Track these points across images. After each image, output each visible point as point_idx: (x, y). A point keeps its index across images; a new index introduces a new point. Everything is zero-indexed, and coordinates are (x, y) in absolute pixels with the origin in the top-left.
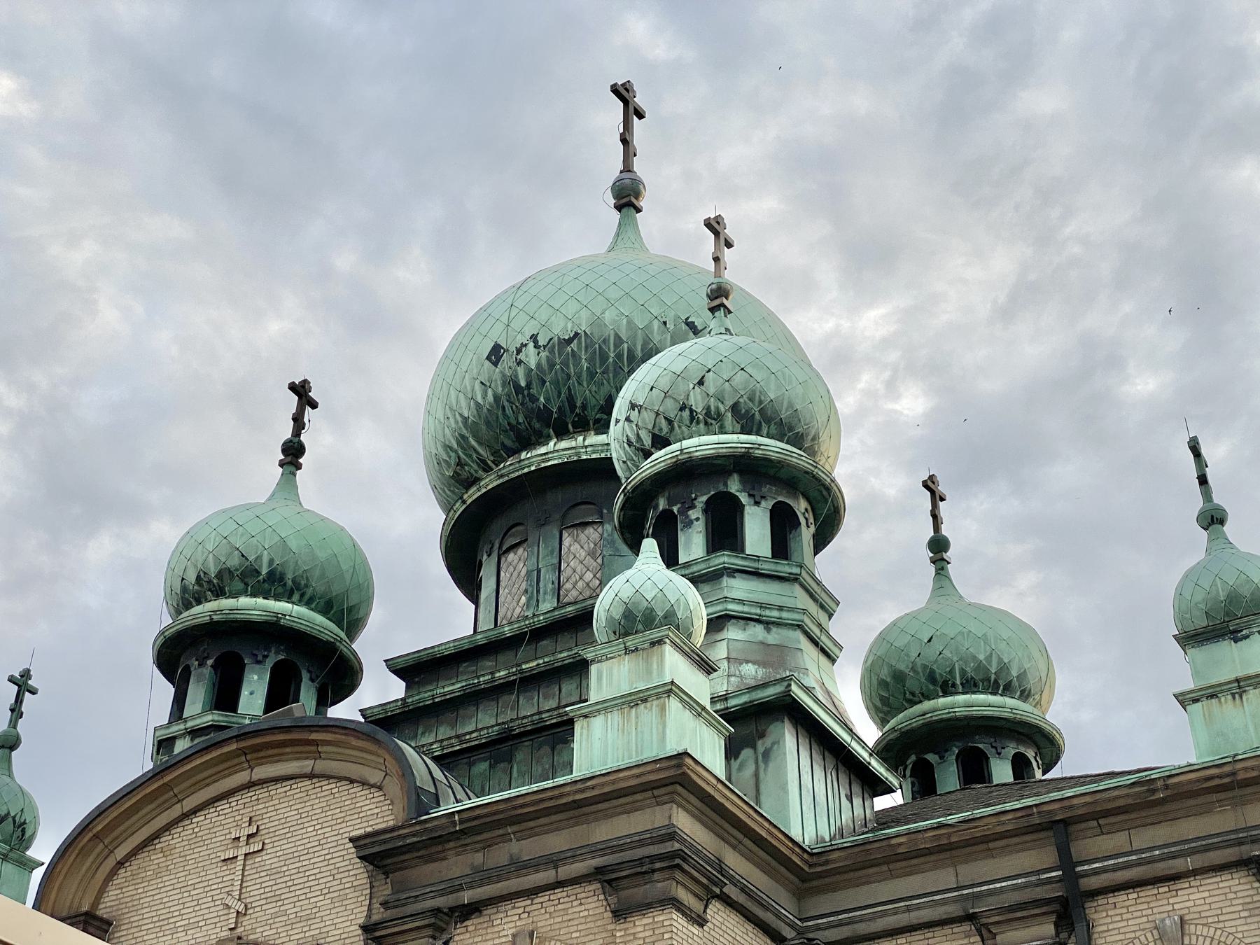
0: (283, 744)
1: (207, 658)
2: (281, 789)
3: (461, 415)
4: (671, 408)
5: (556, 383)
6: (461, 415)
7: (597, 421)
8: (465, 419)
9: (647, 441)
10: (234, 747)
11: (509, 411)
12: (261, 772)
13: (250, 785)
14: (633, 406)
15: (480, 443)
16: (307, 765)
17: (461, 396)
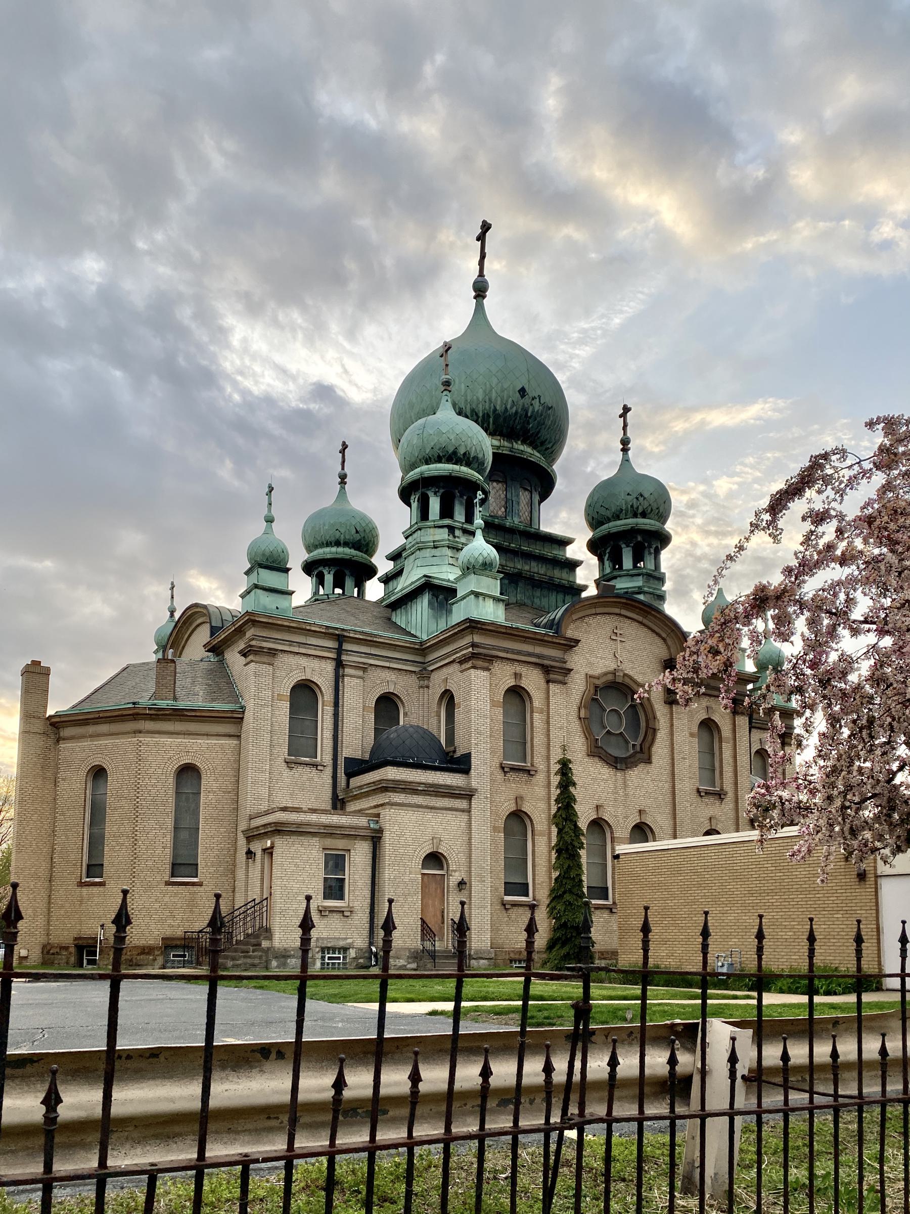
0: (637, 608)
1: (464, 495)
2: (629, 621)
3: (494, 407)
4: (655, 506)
5: (539, 423)
6: (494, 407)
7: (536, 445)
8: (495, 410)
9: (640, 510)
10: (625, 601)
11: (517, 421)
12: (624, 612)
13: (620, 615)
14: (641, 495)
15: (494, 423)
16: (640, 619)
17: (499, 399)
